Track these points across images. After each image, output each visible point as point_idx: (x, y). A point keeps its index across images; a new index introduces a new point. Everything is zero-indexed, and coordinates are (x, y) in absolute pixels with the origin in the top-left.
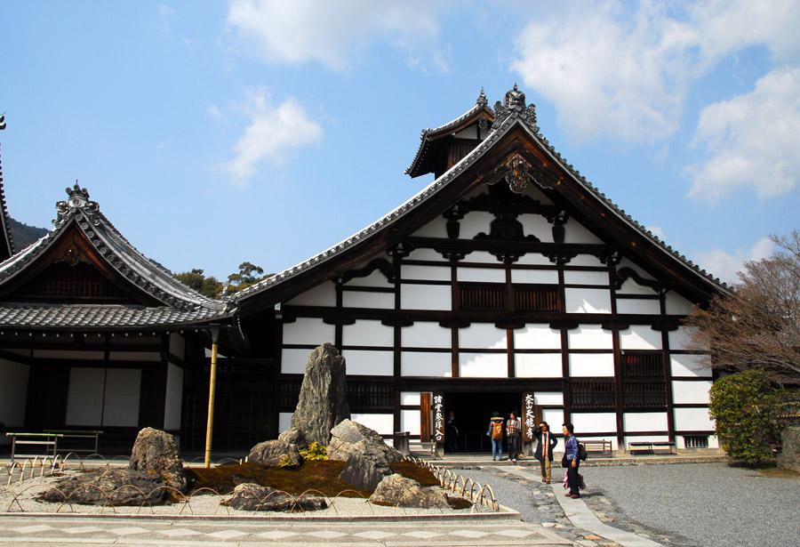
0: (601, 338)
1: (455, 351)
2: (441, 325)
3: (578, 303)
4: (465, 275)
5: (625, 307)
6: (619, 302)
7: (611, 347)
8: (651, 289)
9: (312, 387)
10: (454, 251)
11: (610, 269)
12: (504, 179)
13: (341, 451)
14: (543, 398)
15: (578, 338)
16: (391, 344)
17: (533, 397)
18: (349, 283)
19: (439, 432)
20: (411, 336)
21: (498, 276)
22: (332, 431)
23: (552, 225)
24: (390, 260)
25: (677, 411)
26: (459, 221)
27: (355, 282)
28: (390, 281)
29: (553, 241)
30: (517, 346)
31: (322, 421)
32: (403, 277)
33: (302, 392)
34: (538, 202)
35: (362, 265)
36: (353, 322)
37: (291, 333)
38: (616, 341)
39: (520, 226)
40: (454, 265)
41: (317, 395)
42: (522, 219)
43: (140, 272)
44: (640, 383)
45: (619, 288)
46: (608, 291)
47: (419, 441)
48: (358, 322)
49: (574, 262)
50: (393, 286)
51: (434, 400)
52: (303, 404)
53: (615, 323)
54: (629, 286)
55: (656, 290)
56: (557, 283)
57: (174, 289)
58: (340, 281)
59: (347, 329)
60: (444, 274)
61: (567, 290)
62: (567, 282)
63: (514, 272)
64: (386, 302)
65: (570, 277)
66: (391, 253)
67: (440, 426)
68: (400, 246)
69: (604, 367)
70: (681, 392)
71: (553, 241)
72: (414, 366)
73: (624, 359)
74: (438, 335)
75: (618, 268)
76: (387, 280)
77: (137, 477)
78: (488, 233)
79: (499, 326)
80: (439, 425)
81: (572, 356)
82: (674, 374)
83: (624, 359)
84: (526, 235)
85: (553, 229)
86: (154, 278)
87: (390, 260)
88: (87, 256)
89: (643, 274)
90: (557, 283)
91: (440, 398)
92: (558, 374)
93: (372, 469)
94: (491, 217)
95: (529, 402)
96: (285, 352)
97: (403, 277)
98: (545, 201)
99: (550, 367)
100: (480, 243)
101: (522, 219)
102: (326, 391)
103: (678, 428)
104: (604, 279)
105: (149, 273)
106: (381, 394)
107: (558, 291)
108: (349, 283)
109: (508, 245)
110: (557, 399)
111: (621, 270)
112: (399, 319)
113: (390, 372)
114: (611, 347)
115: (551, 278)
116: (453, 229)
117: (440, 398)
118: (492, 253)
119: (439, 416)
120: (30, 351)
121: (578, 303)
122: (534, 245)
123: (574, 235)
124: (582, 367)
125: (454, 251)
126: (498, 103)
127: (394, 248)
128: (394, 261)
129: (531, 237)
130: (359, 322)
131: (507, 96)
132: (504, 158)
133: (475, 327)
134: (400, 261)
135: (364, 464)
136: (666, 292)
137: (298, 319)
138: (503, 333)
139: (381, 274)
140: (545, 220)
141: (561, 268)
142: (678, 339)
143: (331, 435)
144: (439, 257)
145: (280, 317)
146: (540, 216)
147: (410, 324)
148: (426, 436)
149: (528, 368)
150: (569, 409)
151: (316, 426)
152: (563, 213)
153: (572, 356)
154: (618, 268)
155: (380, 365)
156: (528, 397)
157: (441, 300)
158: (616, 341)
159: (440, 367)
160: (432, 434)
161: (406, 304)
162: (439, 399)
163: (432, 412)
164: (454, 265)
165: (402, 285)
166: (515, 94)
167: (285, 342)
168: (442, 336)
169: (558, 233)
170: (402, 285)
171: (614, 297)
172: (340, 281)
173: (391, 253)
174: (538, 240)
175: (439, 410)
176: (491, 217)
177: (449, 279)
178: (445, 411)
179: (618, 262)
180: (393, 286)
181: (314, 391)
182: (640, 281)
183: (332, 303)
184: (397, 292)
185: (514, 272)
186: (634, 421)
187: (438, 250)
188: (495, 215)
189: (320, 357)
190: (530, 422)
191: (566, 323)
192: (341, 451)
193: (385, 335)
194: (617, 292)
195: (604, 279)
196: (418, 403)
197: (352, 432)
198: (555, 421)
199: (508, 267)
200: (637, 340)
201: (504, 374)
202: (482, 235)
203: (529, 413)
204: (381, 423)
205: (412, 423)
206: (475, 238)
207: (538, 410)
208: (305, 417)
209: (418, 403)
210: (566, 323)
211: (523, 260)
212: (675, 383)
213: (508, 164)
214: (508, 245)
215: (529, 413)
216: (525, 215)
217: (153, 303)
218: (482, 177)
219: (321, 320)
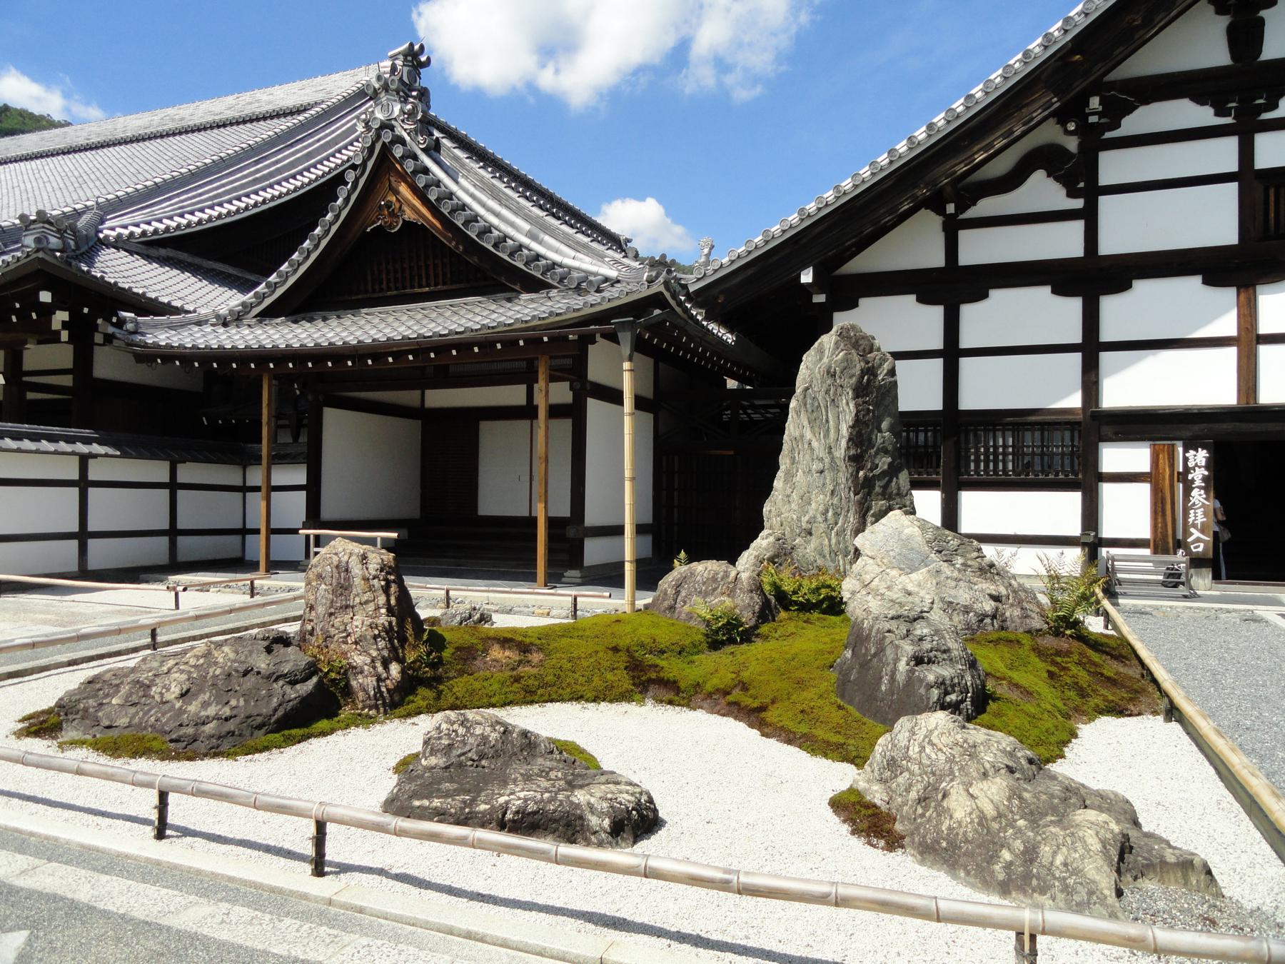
2: (1206, 282)
9: (808, 435)
13: (876, 593)
16: (1077, 338)
18: (972, 213)
19: (1196, 534)
22: (859, 541)
24: (1072, 144)
26: (1263, 13)
27: (988, 206)
28: (1072, 194)
31: (837, 515)
33: (785, 447)
35: (1002, 166)
41: (821, 452)
43: (503, 227)
47: (1146, 552)
48: (995, 294)
50: (1078, 203)
51: (1186, 460)
52: (790, 475)
57: (572, 253)
58: (951, 208)
60: (1222, 154)
66: (1071, 127)
68: (1095, 103)
76: (1064, 192)
77: (242, 669)
86: (533, 237)
87: (1072, 144)
88: (414, 208)
93: (902, 666)
97: (1105, 179)
102: (843, 443)
105: (526, 226)
106: (1058, 451)
108: (972, 213)
112: (1092, 278)
119: (1198, 496)
120: (417, 393)
127: (1081, 116)
128: (1080, 145)
130: (996, 295)
134: (1094, 142)
135: (881, 650)
137: (863, 302)
139: (1051, 181)
143: (857, 553)
145: (820, 298)
148: (1165, 538)
151: (820, 527)
161: (1109, 245)
162: (1200, 457)
163: (1180, 487)
170: (1105, 202)
172: (951, 208)
173: (1071, 127)
175: (1198, 483)
177: (1232, 166)
178: (1219, 483)
180: (1078, 203)
181: (815, 444)
183: (936, 259)
184: (1090, 217)
187: (1199, 100)
189: (825, 360)
192: (876, 593)
193: (1058, 316)
196: (1145, 467)
197: (906, 542)
205: (1127, 512)
208: (793, 506)
209: (1145, 467)
217: (535, 285)
219: (913, 298)
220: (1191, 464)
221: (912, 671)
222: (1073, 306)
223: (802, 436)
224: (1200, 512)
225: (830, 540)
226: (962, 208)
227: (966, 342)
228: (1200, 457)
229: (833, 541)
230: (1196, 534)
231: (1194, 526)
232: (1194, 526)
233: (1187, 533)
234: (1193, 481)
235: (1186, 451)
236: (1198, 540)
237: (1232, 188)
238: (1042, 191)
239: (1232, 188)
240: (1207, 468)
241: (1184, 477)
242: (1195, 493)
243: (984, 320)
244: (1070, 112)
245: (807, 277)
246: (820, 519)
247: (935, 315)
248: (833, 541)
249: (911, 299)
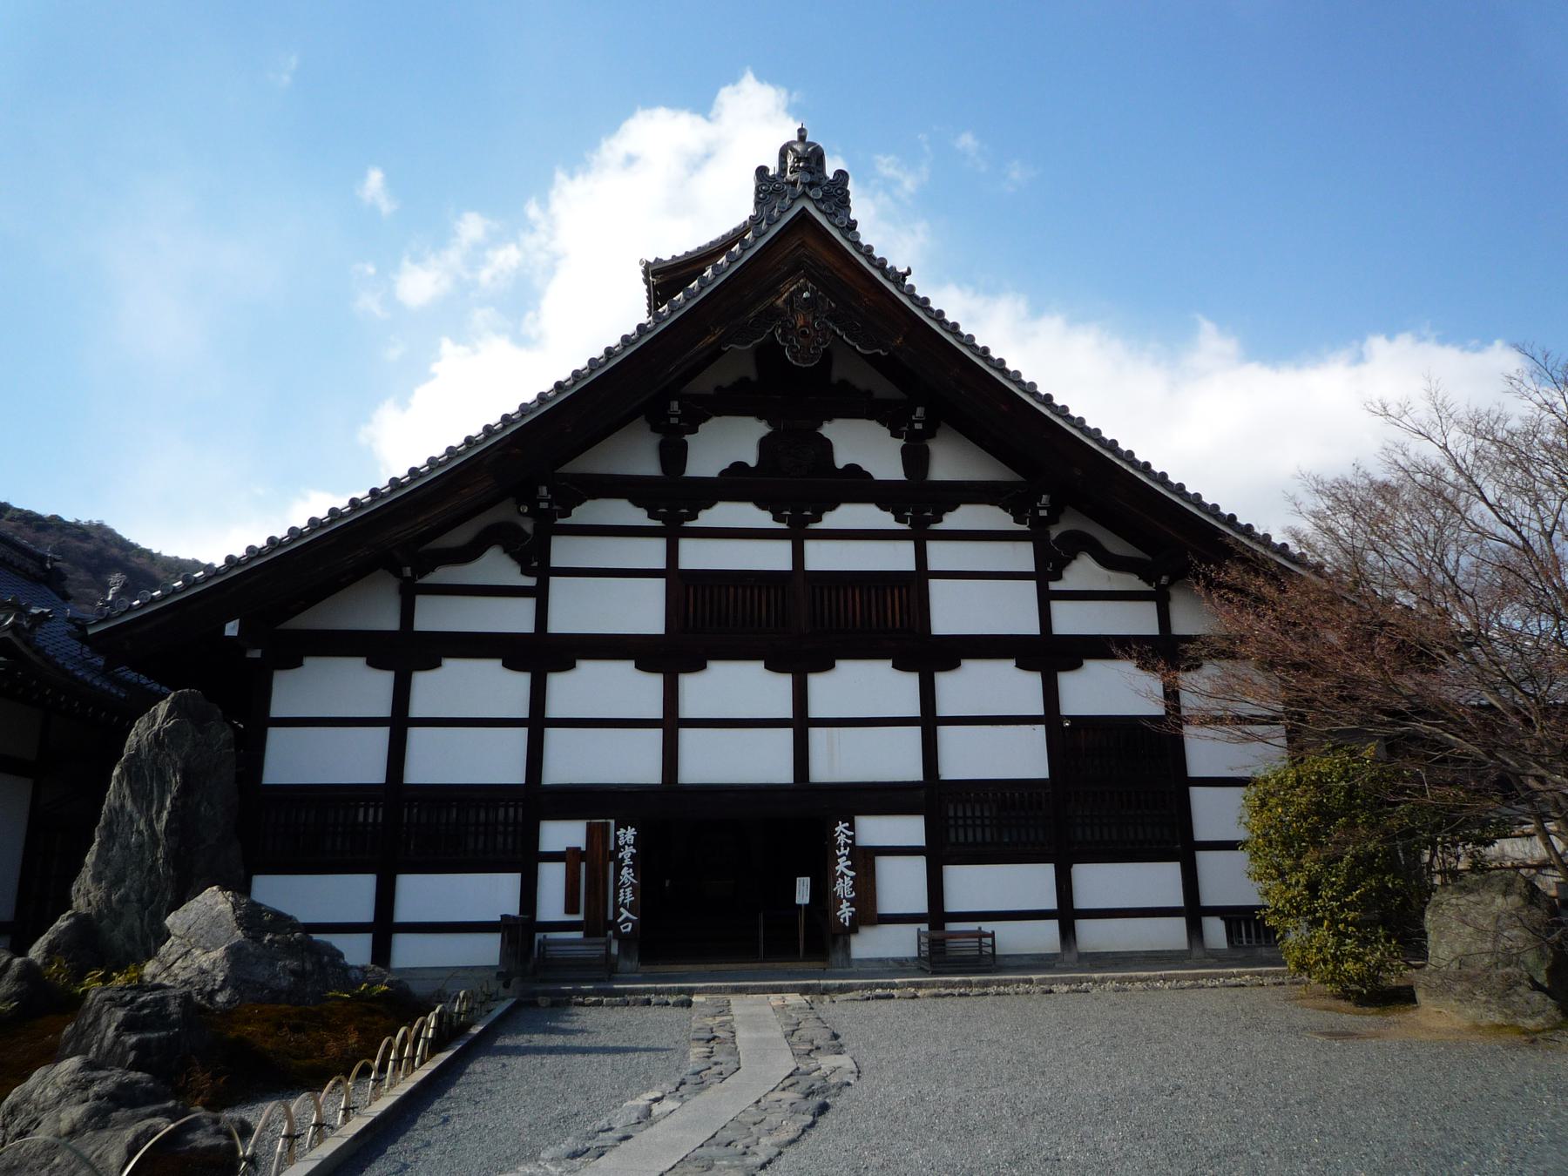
0: (1016, 688)
1: (671, 723)
3: (952, 610)
4: (697, 555)
5: (1070, 620)
6: (1057, 607)
7: (1038, 709)
8: (1135, 578)
10: (674, 503)
11: (1036, 536)
12: (772, 333)
14: (874, 830)
15: (959, 689)
17: (852, 828)
19: (625, 914)
20: (573, 690)
21: (774, 557)
23: (902, 442)
24: (528, 526)
25: (1204, 859)
26: (687, 438)
28: (526, 572)
29: (903, 478)
30: (815, 711)
32: (556, 561)
34: (869, 393)
36: (438, 665)
37: (294, 692)
38: (1051, 694)
39: (827, 446)
40: (673, 533)
42: (829, 430)
44: (1112, 792)
45: (1058, 577)
46: (1033, 583)
47: (578, 935)
49: (951, 521)
50: (531, 582)
51: (617, 838)
53: (1047, 654)
54: (1083, 573)
55: (1146, 578)
56: (913, 568)
58: (408, 571)
59: (422, 681)
60: (651, 553)
61: (935, 585)
62: (934, 564)
63: (811, 547)
64: (516, 617)
65: (941, 555)
67: (629, 898)
69: (1023, 757)
70: (1214, 813)
71: (903, 478)
72: (573, 760)
73: (1068, 736)
74: (632, 689)
75: (1055, 532)
76: (518, 569)
78: (752, 462)
79: (774, 666)
80: (627, 896)
81: (944, 732)
82: (1196, 768)
83: (1068, 736)
84: (840, 463)
85: (905, 451)
87: (528, 526)
89: (1116, 545)
90: (913, 568)
91: (631, 831)
92: (912, 771)
94: (760, 429)
95: (842, 839)
96: (275, 735)
97: (556, 561)
98: (885, 389)
99: (896, 757)
100: (735, 483)
101: (829, 430)
103: (1209, 898)
104: (1021, 556)
107: (914, 585)
109: (797, 486)
110: (911, 829)
111: (1063, 536)
112: (541, 654)
113: (515, 774)
114: (1038, 709)
115: (897, 557)
116: (674, 455)
117: (631, 831)
118: (762, 505)
121: (952, 610)
122: (858, 486)
123: (950, 462)
124: (969, 757)
125: (674, 503)
126: (761, 171)
127: (533, 502)
128: (535, 528)
129: (853, 470)
130: (451, 666)
131: (783, 154)
132: (773, 290)
133: (719, 671)
134: (549, 528)
136: (1171, 583)
138: (783, 684)
140: (886, 432)
141: (920, 536)
142: (1200, 687)
144: (638, 516)
146: (874, 424)
147: (568, 666)
149: (839, 759)
150: (939, 854)
152: (920, 411)
153: (944, 732)
154: (1055, 532)
155: (496, 761)
156: (841, 827)
157: (642, 610)
158: (1051, 694)
159: (633, 761)
160: (610, 917)
161: (559, 623)
162: (628, 835)
164: (673, 533)
165: (555, 581)
166: (799, 148)
167: (276, 711)
168: (638, 691)
169: (915, 459)
170: (555, 581)
171: (1045, 599)
172: (408, 571)
174: (868, 475)
175: (627, 861)
176: (760, 429)
177: (660, 563)
179: (1053, 519)
180: (531, 582)
182: (1108, 561)
183: (389, 621)
184: (541, 596)
185: (811, 547)
186: (1097, 882)
187: (637, 502)
188: (770, 424)
190: (844, 887)
191: (930, 655)
193: (506, 690)
194: (1054, 586)
195: (1021, 556)
198: (902, 885)
199: (798, 534)
200: (1108, 691)
201: (783, 773)
202: (738, 467)
203: (842, 865)
204: (494, 894)
206: (723, 473)
207: (865, 859)
210: (930, 655)
211: (831, 520)
212: (1198, 795)
213: (779, 302)
214: (797, 486)
215: (842, 865)
216: (838, 422)
218: (719, 332)
220: (621, 843)
221: (118, 1037)
222: (522, 681)
223: (122, 806)
224: (629, 890)
225: (142, 921)
226: (423, 574)
227: (416, 711)
228: (628, 835)
229: (146, 919)
230: (625, 914)
231: (624, 905)
232: (624, 905)
233: (617, 914)
234: (623, 859)
235: (617, 829)
236: (627, 920)
237: (660, 583)
238: (497, 567)
239: (660, 583)
240: (634, 846)
241: (614, 855)
242: (624, 871)
243: (435, 690)
244: (525, 494)
245: (232, 629)
246: (133, 897)
247: (383, 681)
248: (146, 919)
249: (362, 661)
